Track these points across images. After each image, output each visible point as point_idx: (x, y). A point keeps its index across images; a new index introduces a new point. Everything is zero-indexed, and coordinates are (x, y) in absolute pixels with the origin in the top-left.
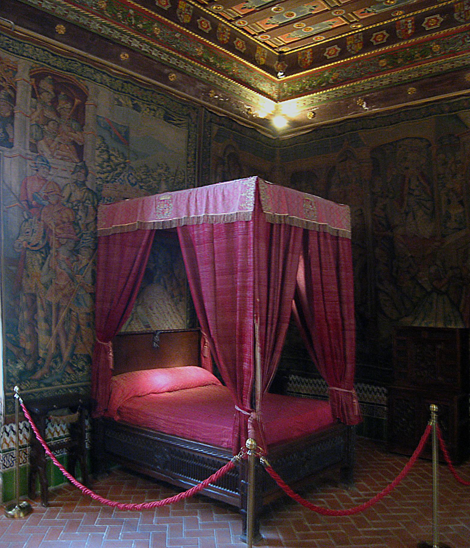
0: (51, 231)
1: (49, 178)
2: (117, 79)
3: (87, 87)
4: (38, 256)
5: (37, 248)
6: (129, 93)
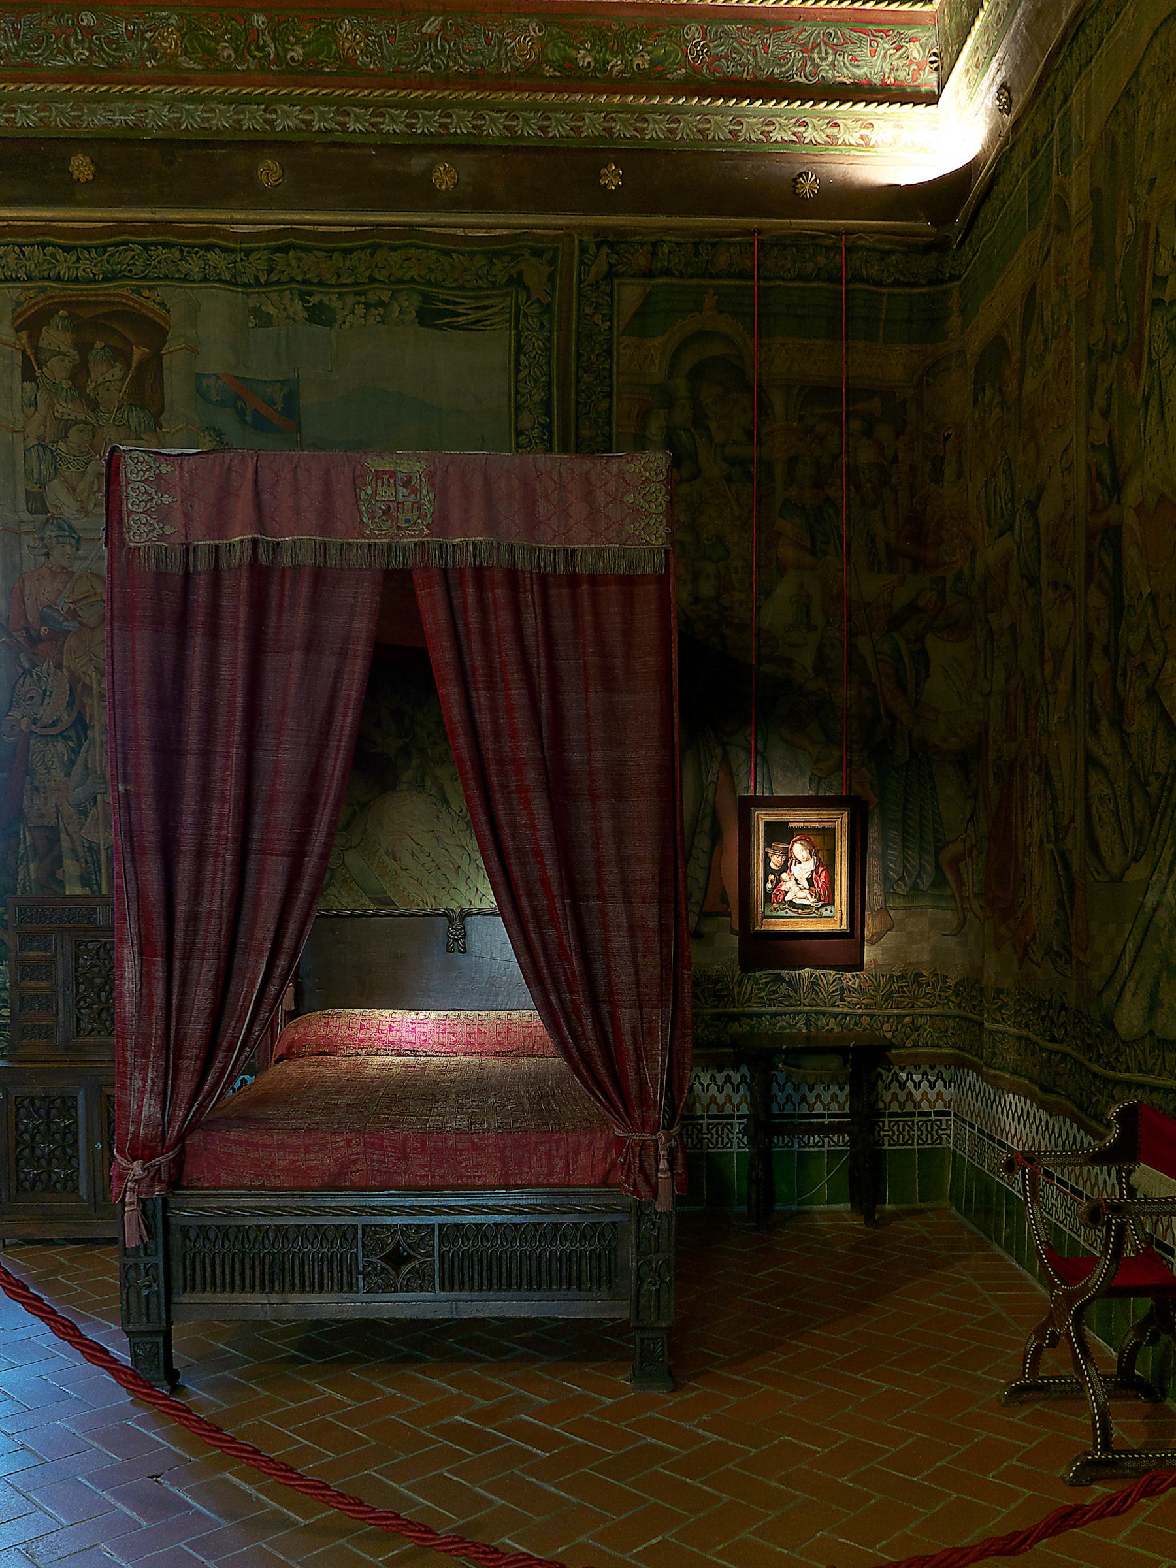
0: (87, 689)
1: (77, 567)
2: (252, 250)
3: (162, 305)
4: (60, 747)
5: (52, 731)
6: (292, 280)
